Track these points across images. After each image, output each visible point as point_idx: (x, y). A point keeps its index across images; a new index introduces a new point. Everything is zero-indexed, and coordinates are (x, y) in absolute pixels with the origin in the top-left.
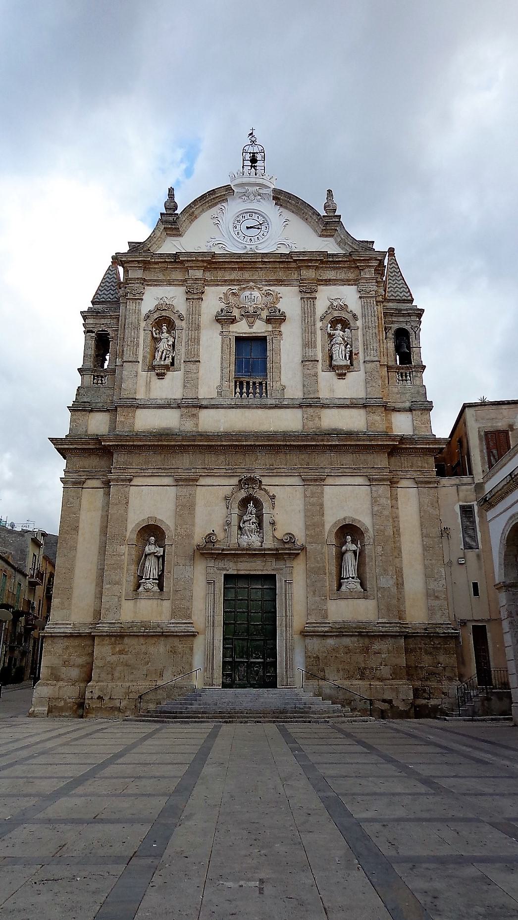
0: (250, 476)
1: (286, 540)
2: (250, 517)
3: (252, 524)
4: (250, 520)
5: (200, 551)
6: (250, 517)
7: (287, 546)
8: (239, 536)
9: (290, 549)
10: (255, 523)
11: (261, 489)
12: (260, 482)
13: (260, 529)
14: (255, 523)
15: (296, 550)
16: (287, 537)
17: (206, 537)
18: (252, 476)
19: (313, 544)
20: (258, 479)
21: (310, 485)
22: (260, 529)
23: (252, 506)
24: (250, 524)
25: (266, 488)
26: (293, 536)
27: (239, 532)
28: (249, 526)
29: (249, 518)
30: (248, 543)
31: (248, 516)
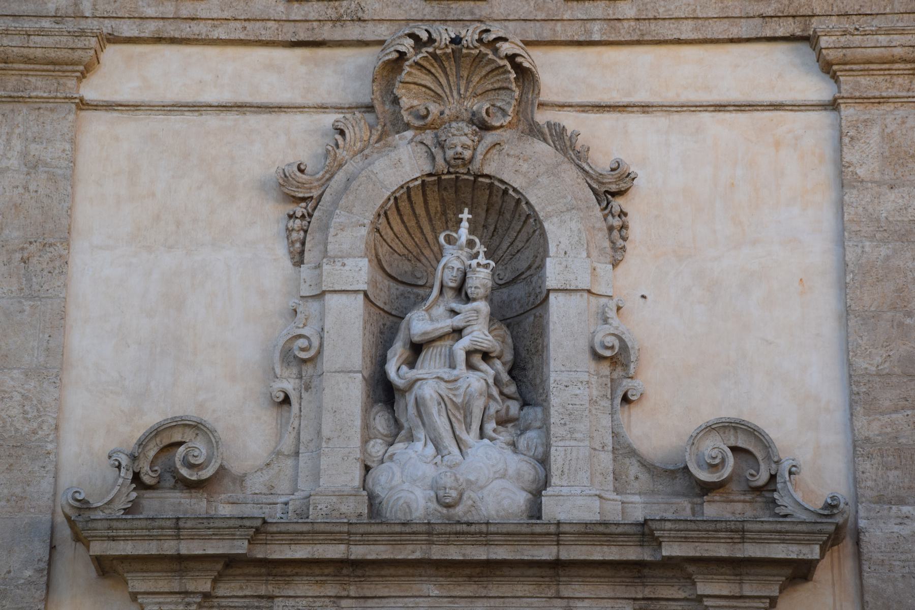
0: (456, 41)
1: (713, 467)
2: (454, 313)
3: (470, 366)
4: (458, 332)
5: (98, 548)
6: (454, 313)
7: (712, 510)
8: (377, 448)
9: (740, 533)
10: (486, 356)
11: (534, 131)
12: (525, 75)
13: (525, 404)
14: (486, 356)
15: (783, 537)
16: (713, 446)
17: (142, 444)
18: (470, 35)
19: (905, 509)
20: (511, 58)
21: (881, 100)
22: (525, 404)
23: (471, 244)
24: (452, 366)
25: (569, 121)
26: (753, 432)
27: (381, 422)
28: (445, 373)
29: (446, 324)
30: (435, 486)
31: (440, 310)
